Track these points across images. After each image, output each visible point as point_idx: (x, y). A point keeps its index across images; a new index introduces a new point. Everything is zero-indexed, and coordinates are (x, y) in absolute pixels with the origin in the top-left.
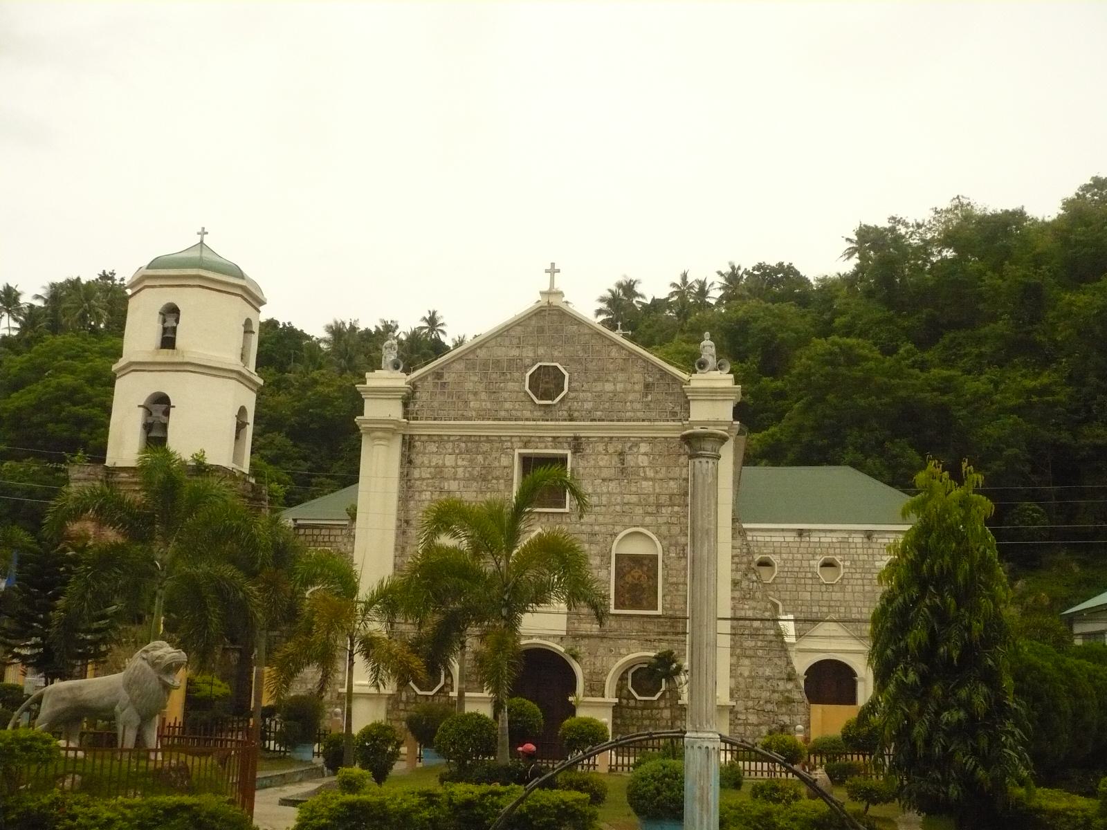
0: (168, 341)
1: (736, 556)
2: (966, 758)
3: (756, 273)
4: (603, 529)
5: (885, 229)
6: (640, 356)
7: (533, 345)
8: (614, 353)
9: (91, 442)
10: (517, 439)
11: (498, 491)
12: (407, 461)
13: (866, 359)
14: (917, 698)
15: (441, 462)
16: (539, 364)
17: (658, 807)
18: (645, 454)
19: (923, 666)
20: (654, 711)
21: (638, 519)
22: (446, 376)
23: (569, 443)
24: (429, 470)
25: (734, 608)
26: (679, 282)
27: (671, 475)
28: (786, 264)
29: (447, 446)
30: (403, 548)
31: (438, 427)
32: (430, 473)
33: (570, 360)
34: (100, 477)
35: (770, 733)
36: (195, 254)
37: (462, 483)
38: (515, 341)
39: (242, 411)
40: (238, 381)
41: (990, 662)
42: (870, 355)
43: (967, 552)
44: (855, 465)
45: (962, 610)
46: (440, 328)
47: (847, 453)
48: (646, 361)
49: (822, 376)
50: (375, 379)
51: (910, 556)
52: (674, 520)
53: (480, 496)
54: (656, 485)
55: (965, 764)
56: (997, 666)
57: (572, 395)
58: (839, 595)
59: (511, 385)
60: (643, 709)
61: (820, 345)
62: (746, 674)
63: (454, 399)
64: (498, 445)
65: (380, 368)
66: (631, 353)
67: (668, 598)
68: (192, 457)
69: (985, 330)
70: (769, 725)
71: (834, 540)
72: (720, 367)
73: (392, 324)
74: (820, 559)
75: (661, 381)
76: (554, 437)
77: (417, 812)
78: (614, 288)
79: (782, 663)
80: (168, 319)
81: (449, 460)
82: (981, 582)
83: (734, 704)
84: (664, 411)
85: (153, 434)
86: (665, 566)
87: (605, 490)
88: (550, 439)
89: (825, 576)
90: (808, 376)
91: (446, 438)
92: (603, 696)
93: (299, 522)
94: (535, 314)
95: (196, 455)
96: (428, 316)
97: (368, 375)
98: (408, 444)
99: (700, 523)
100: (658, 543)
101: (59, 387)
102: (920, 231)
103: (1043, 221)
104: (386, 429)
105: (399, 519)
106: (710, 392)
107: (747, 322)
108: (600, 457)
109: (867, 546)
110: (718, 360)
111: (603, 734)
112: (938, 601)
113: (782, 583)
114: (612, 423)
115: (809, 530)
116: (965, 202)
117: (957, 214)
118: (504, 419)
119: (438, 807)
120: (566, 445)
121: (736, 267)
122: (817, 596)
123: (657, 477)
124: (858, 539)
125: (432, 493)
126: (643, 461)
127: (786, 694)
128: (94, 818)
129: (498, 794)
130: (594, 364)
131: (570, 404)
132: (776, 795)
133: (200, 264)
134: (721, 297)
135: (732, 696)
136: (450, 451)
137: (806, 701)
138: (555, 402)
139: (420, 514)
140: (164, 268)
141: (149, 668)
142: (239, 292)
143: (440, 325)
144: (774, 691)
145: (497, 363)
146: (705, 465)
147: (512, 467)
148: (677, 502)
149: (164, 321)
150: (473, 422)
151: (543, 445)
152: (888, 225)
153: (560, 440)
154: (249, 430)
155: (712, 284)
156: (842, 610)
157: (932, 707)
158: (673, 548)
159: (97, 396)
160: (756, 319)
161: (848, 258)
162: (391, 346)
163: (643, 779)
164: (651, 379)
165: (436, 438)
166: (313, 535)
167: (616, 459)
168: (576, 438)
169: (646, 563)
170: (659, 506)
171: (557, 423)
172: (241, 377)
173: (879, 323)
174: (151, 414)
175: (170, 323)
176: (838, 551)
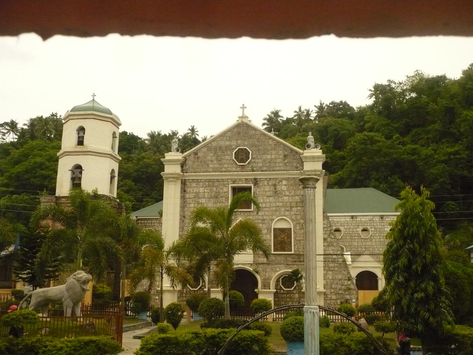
0: (80, 142)
1: (325, 228)
2: (425, 313)
3: (331, 105)
4: (268, 218)
5: (386, 85)
6: (282, 143)
7: (236, 140)
9: (49, 186)
10: (230, 180)
12: (184, 191)
13: (378, 141)
14: (403, 288)
16: (239, 148)
18: (285, 185)
20: (291, 295)
22: (199, 154)
23: (252, 181)
24: (193, 194)
25: (324, 250)
26: (298, 110)
28: (343, 101)
32: (193, 196)
33: (252, 146)
34: (54, 201)
35: (341, 303)
36: (91, 105)
38: (228, 138)
39: (113, 171)
40: (110, 158)
41: (434, 272)
42: (381, 140)
43: (424, 225)
44: (374, 187)
45: (422, 250)
46: (196, 133)
50: (169, 156)
51: (399, 227)
52: (298, 213)
53: (215, 205)
55: (425, 316)
56: (438, 273)
57: (253, 161)
59: (227, 157)
60: (287, 294)
61: (359, 136)
62: (330, 278)
64: (222, 183)
65: (171, 151)
66: (278, 142)
67: (296, 246)
68: (92, 191)
69: (430, 127)
70: (341, 300)
71: (367, 220)
72: (316, 147)
73: (176, 132)
74: (361, 228)
75: (291, 154)
76: (246, 179)
77: (191, 341)
78: (270, 114)
79: (346, 273)
80: (80, 133)
81: (201, 190)
82: (430, 237)
83: (325, 291)
85: (76, 182)
89: (363, 235)
90: (355, 149)
91: (200, 180)
92: (270, 289)
95: (94, 190)
96: (191, 128)
97: (166, 154)
98: (184, 183)
99: (308, 216)
100: (291, 223)
101: (35, 163)
102: (401, 86)
103: (454, 80)
104: (174, 177)
106: (313, 158)
108: (265, 187)
110: (315, 144)
111: (269, 305)
112: (411, 246)
113: (345, 239)
114: (270, 172)
115: (356, 216)
116: (420, 72)
117: (417, 78)
118: (224, 172)
120: (251, 182)
121: (322, 103)
122: (360, 244)
123: (290, 195)
124: (377, 219)
125: (195, 204)
126: (284, 188)
127: (348, 286)
128: (54, 347)
129: (226, 333)
130: (262, 147)
131: (252, 164)
132: (344, 330)
133: (93, 109)
134: (316, 116)
135: (324, 288)
136: (202, 186)
137: (357, 289)
138: (246, 164)
140: (77, 111)
141: (76, 282)
142: (110, 120)
144: (342, 285)
145: (220, 148)
146: (310, 191)
147: (228, 192)
148: (299, 205)
149: (79, 134)
150: (211, 173)
151: (241, 182)
152: (387, 84)
153: (248, 180)
154: (116, 179)
155: (312, 111)
156: (371, 249)
157: (410, 291)
158: (298, 225)
159: (51, 166)
160: (331, 126)
161: (370, 98)
162: (175, 142)
163: (287, 325)
164: (286, 153)
165: (195, 181)
166: (144, 223)
167: (272, 188)
168: (255, 179)
169: (286, 232)
170: (291, 207)
171: (247, 173)
172: (112, 156)
173: (384, 126)
174: (74, 173)
175: (81, 134)
176: (369, 224)
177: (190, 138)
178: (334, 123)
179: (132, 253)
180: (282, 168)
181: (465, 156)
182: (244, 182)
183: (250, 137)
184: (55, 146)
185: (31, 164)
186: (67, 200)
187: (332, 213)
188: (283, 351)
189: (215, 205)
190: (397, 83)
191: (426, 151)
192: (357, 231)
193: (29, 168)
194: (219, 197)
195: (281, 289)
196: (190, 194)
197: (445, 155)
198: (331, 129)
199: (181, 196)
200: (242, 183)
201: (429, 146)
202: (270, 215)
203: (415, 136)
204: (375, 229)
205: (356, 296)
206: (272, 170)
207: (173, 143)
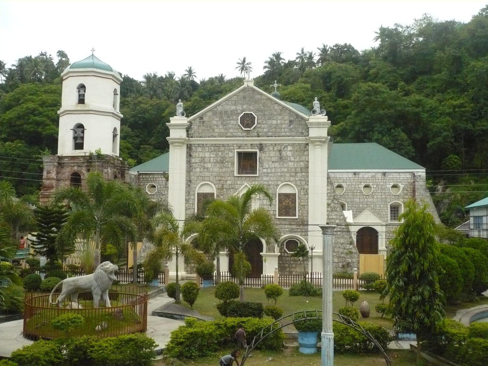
0: (81, 101)
3: (335, 48)
5: (392, 29)
6: (287, 109)
7: (241, 104)
8: (276, 107)
10: (236, 145)
11: (228, 167)
12: (189, 155)
13: (383, 92)
14: (403, 291)
15: (203, 155)
17: (305, 327)
18: (290, 151)
19: (405, 279)
21: (287, 179)
22: (204, 118)
25: (328, 215)
26: (300, 52)
28: (348, 44)
30: (189, 192)
32: (199, 160)
33: (258, 111)
34: (56, 161)
35: (343, 266)
36: (90, 61)
37: (213, 164)
38: (233, 103)
39: (115, 129)
41: (431, 278)
42: (385, 91)
43: (423, 235)
44: (378, 141)
46: (193, 74)
48: (290, 111)
50: (174, 120)
51: (401, 236)
52: (303, 179)
53: (220, 170)
56: (433, 279)
57: (258, 126)
58: (372, 199)
59: (232, 122)
61: (364, 86)
64: (227, 148)
65: (176, 115)
67: (301, 211)
69: (436, 77)
71: (369, 176)
72: (322, 113)
74: (363, 184)
76: (251, 144)
78: (271, 56)
79: (348, 237)
80: (81, 91)
81: (207, 155)
84: (298, 132)
85: (79, 141)
86: (299, 198)
89: (365, 192)
90: (358, 101)
91: (205, 145)
92: (274, 252)
96: (188, 70)
97: (171, 118)
98: (189, 148)
101: (27, 108)
102: (408, 30)
103: (464, 24)
104: (180, 142)
105: (187, 180)
107: (331, 73)
108: (271, 152)
112: (411, 254)
115: (359, 172)
116: (429, 16)
118: (230, 137)
119: (222, 328)
121: (326, 45)
122: (362, 200)
124: (379, 176)
126: (289, 154)
128: (100, 346)
129: (243, 322)
130: (268, 112)
132: (348, 314)
133: (93, 66)
134: (319, 59)
138: (251, 129)
142: (111, 77)
144: (345, 249)
145: (226, 112)
146: (328, 238)
147: (234, 157)
149: (79, 92)
151: (246, 148)
152: (394, 27)
154: (118, 137)
155: (315, 54)
156: (372, 206)
157: (409, 294)
158: (302, 190)
159: (45, 112)
160: (335, 72)
161: (376, 41)
162: (180, 105)
164: (292, 118)
167: (278, 153)
168: (261, 144)
169: (291, 197)
170: (296, 173)
171: (252, 138)
172: (114, 115)
173: (389, 72)
175: (82, 92)
176: (371, 181)
177: (187, 81)
178: (337, 69)
179: (144, 226)
180: (288, 134)
181: (470, 110)
183: (256, 102)
184: (47, 90)
185: (23, 110)
188: (293, 332)
191: (431, 102)
192: (359, 188)
193: (21, 114)
194: (225, 162)
195: (285, 252)
197: (450, 108)
198: (334, 76)
199: (187, 160)
200: (248, 149)
201: (434, 96)
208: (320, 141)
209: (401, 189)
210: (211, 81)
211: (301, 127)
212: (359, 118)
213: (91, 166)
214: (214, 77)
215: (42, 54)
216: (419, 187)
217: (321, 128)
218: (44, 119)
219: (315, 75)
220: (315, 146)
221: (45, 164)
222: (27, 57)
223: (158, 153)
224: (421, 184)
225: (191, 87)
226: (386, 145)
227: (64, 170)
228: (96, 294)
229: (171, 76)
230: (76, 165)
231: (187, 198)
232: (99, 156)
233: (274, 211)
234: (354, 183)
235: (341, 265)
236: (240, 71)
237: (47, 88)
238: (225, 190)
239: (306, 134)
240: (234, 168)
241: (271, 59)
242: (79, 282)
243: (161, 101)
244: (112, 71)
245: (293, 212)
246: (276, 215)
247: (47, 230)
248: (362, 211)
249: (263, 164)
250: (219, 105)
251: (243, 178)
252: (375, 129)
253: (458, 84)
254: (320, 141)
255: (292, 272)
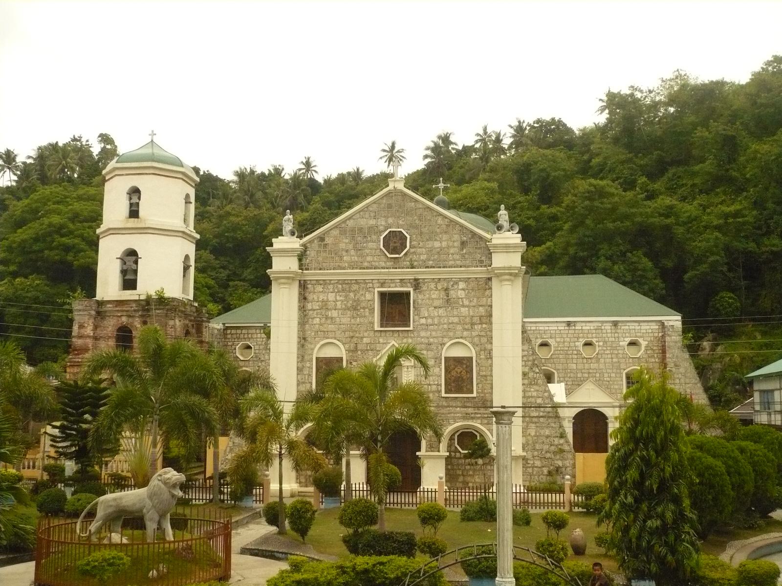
0: (134, 213)
1: (525, 356)
2: (661, 549)
3: (536, 125)
4: (436, 341)
5: (627, 95)
6: (457, 223)
7: (385, 217)
8: (440, 221)
9: (75, 263)
10: (377, 281)
11: (365, 317)
12: (303, 299)
13: (613, 195)
14: (633, 511)
15: (325, 298)
17: (480, 571)
18: (463, 289)
19: (636, 492)
21: (459, 334)
22: (327, 239)
23: (411, 283)
25: (524, 391)
26: (481, 132)
27: (481, 304)
28: (557, 119)
29: (329, 287)
31: (322, 274)
32: (319, 306)
33: (411, 227)
34: (94, 308)
35: (550, 473)
36: (148, 151)
38: (372, 214)
39: (187, 257)
40: (182, 237)
41: (676, 490)
42: (616, 192)
43: (662, 422)
44: (606, 273)
45: (660, 458)
46: (313, 169)
47: (600, 262)
48: (462, 226)
49: (583, 208)
50: (279, 243)
51: (628, 425)
52: (483, 333)
53: (352, 320)
54: (471, 310)
55: (661, 552)
56: (680, 493)
57: (412, 250)
59: (371, 245)
61: (583, 185)
62: (533, 434)
63: (333, 255)
64: (363, 285)
65: (283, 236)
67: (480, 386)
68: (156, 293)
69: (697, 168)
70: (548, 467)
71: (592, 328)
72: (511, 229)
74: (582, 341)
77: (336, 579)
78: (436, 140)
81: (331, 296)
82: (671, 441)
83: (525, 454)
84: (474, 259)
85: (127, 277)
86: (478, 364)
87: (436, 314)
88: (398, 281)
89: (586, 352)
91: (328, 282)
92: (439, 451)
93: (226, 325)
94: (385, 196)
96: (304, 161)
97: (274, 240)
98: (303, 286)
99: (502, 462)
100: (472, 348)
101: (50, 225)
102: (652, 95)
103: (739, 85)
104: (289, 277)
105: (299, 337)
106: (506, 247)
107: (529, 165)
108: (432, 292)
109: (613, 331)
111: (443, 513)
112: (644, 453)
113: (557, 358)
116: (683, 73)
118: (367, 268)
119: (348, 574)
121: (522, 121)
122: (580, 366)
123: (471, 304)
124: (608, 327)
125: (320, 319)
126: (461, 294)
127: (559, 447)
129: (382, 564)
131: (411, 257)
132: (551, 549)
133: (152, 158)
134: (512, 144)
135: (524, 449)
137: (573, 450)
138: (401, 256)
139: (313, 334)
140: (127, 162)
141: (163, 486)
142: (180, 176)
143: (313, 166)
144: (551, 445)
145: (361, 229)
146: (504, 429)
147: (373, 300)
149: (130, 199)
150: (346, 271)
151: (394, 285)
152: (628, 92)
153: (405, 281)
154: (192, 270)
155: (505, 134)
156: (598, 375)
157: (641, 516)
158: (483, 352)
159: (78, 229)
160: (536, 163)
161: (601, 113)
164: (465, 238)
165: (321, 282)
167: (443, 293)
168: (416, 280)
169: (465, 363)
170: (473, 324)
171: (403, 270)
172: (185, 235)
173: (623, 162)
174: (125, 263)
175: (135, 200)
176: (594, 335)
177: (303, 180)
178: (540, 159)
179: (231, 411)
180: (458, 263)
181: (751, 220)
182: (398, 284)
184: (82, 195)
185: (44, 226)
186: (116, 306)
187: (537, 317)
188: (464, 580)
189: (352, 320)
190: (644, 91)
191: (690, 209)
192: (576, 347)
193: (40, 233)
195: (456, 451)
196: (313, 303)
199: (299, 306)
200: (396, 287)
201: (694, 198)
202: (440, 337)
203: (673, 180)
204: (605, 342)
205: (572, 462)
206: (442, 265)
207: (285, 221)
208: (511, 274)
209: (643, 349)
210: (342, 179)
211: (479, 251)
212: (575, 236)
213: (149, 316)
214: (345, 172)
215: (74, 140)
216: (671, 344)
217: (509, 254)
218: (76, 241)
219: (505, 168)
220: (501, 281)
221: (76, 313)
222: (50, 145)
223: (256, 294)
224: (675, 339)
225: (308, 188)
226: (617, 279)
227: (105, 322)
228: (151, 520)
229: (278, 172)
230: (125, 314)
231: (300, 365)
232: (162, 301)
233: (438, 385)
234: (568, 339)
235: (545, 471)
236: (387, 163)
237: (81, 192)
238: (359, 352)
239: (487, 262)
240: (373, 317)
241: (435, 143)
242: (124, 501)
243: (261, 211)
244: (182, 166)
245: (468, 387)
246: (441, 391)
247: (77, 418)
248: (580, 383)
249: (420, 310)
250: (350, 218)
251: (388, 334)
252: (602, 252)
253: (731, 180)
254: (511, 274)
255: (468, 483)
